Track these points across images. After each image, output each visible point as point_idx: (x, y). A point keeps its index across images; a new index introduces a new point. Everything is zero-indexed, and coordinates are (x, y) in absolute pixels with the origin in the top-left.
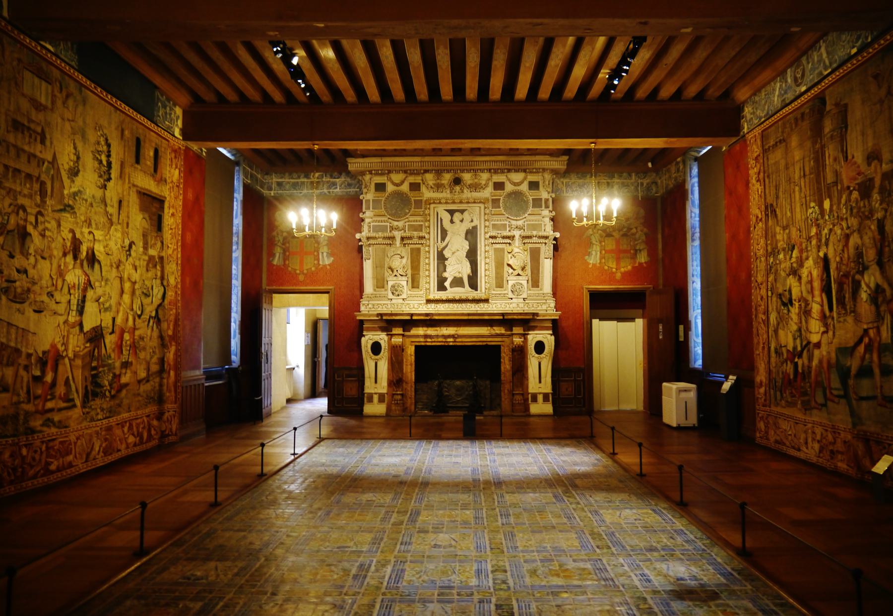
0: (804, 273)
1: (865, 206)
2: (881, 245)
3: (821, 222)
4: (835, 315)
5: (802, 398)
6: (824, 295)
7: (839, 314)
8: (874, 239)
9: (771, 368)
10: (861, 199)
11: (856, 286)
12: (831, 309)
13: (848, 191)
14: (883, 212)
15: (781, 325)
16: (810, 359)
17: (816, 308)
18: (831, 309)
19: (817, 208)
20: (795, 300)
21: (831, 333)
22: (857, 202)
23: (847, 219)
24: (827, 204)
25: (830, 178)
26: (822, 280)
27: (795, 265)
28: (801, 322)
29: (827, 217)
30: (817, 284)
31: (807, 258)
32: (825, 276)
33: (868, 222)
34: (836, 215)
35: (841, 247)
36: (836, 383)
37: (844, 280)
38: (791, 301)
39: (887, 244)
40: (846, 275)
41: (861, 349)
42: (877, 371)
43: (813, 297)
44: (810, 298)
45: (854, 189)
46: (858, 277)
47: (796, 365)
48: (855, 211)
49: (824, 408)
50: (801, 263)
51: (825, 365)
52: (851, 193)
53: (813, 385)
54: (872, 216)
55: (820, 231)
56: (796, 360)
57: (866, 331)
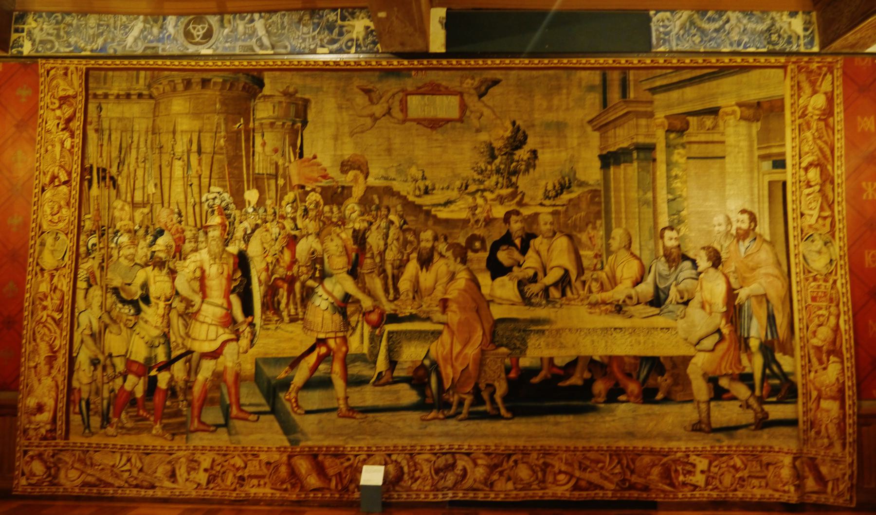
0: (187, 268)
1: (332, 211)
2: (357, 256)
3: (236, 213)
4: (258, 320)
5: (165, 421)
6: (235, 300)
7: (267, 321)
8: (345, 247)
9: (75, 384)
10: (325, 204)
11: (308, 294)
12: (248, 310)
13: (300, 191)
14: (366, 225)
15: (114, 328)
16: (192, 371)
17: (211, 311)
18: (248, 310)
19: (226, 196)
20: (159, 298)
21: (244, 342)
22: (317, 204)
23: (294, 219)
24: (251, 196)
25: (261, 165)
26: (230, 279)
27: (162, 255)
28: (169, 325)
29: (250, 210)
30: (216, 285)
31: (196, 250)
32: (239, 274)
33: (338, 230)
34: (270, 211)
35: (277, 247)
36: (251, 397)
37: (280, 283)
38: (146, 299)
39: (368, 255)
40: (291, 281)
41: (312, 358)
42: (339, 383)
43: (204, 296)
44: (197, 299)
45: (313, 190)
46: (310, 283)
47: (153, 381)
48: (312, 214)
49: (223, 430)
50: (179, 253)
51: (230, 378)
52: (307, 193)
53: (197, 404)
54: (344, 224)
55: (232, 224)
56: (153, 373)
57: (321, 342)
